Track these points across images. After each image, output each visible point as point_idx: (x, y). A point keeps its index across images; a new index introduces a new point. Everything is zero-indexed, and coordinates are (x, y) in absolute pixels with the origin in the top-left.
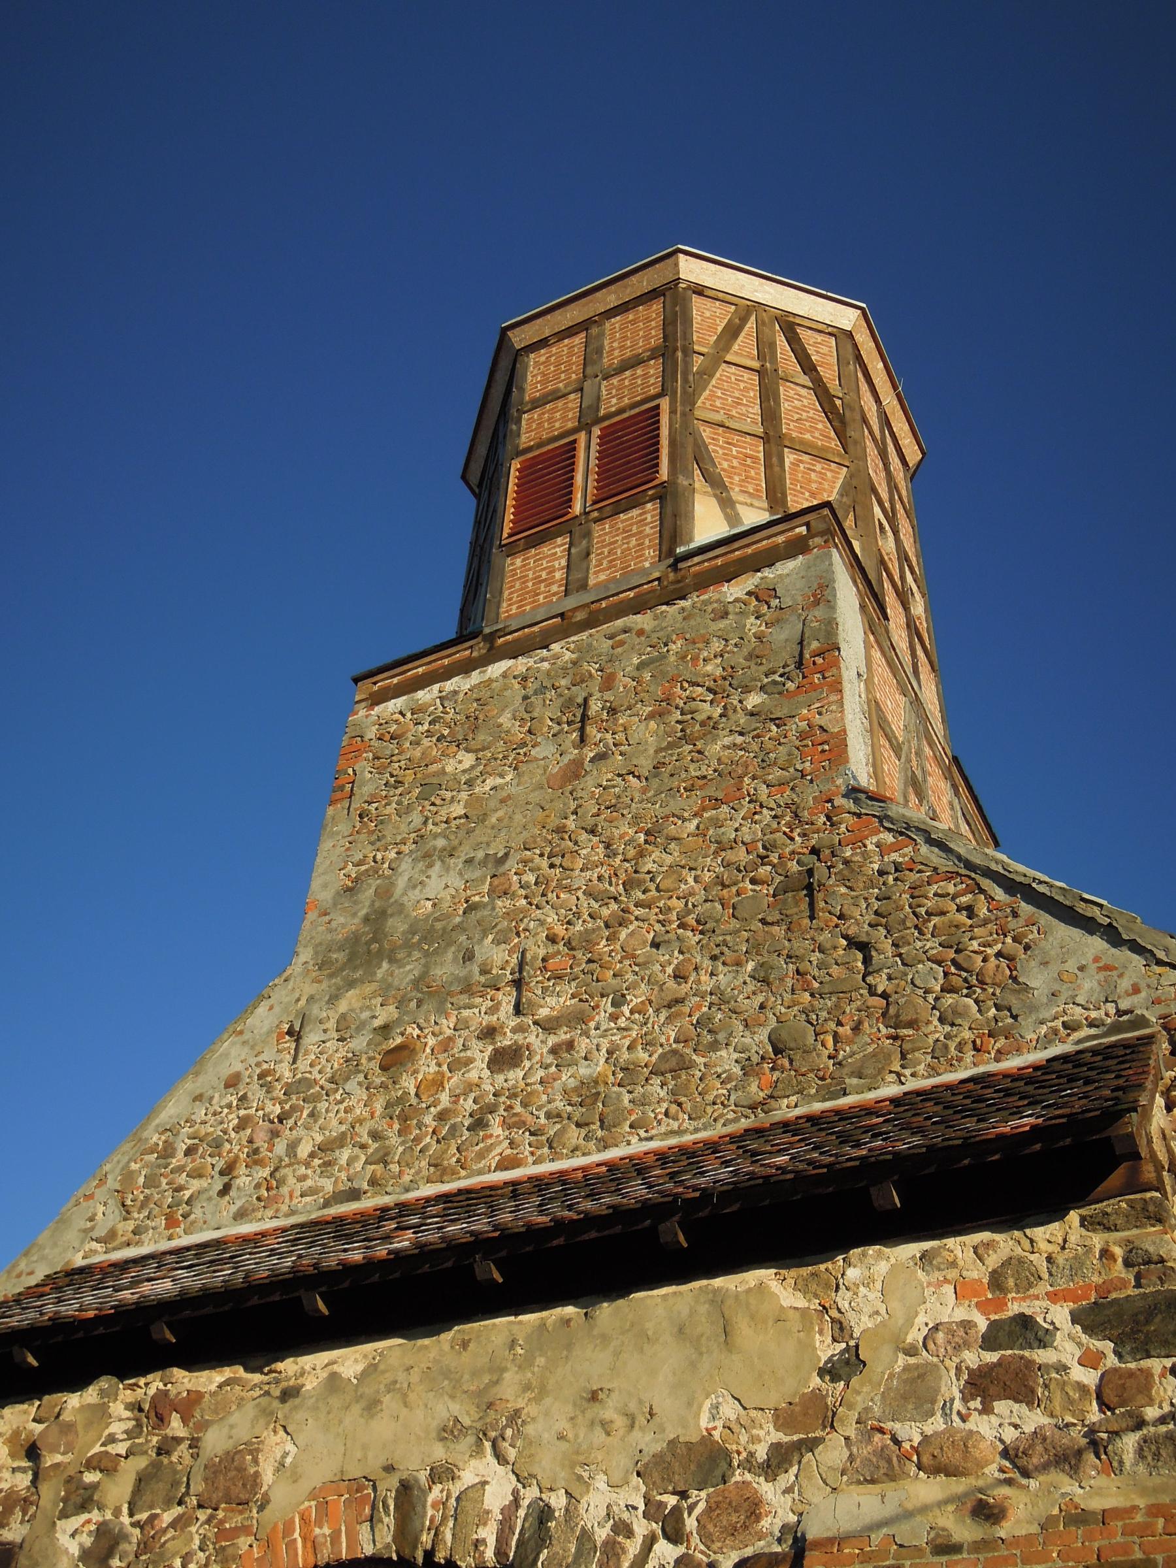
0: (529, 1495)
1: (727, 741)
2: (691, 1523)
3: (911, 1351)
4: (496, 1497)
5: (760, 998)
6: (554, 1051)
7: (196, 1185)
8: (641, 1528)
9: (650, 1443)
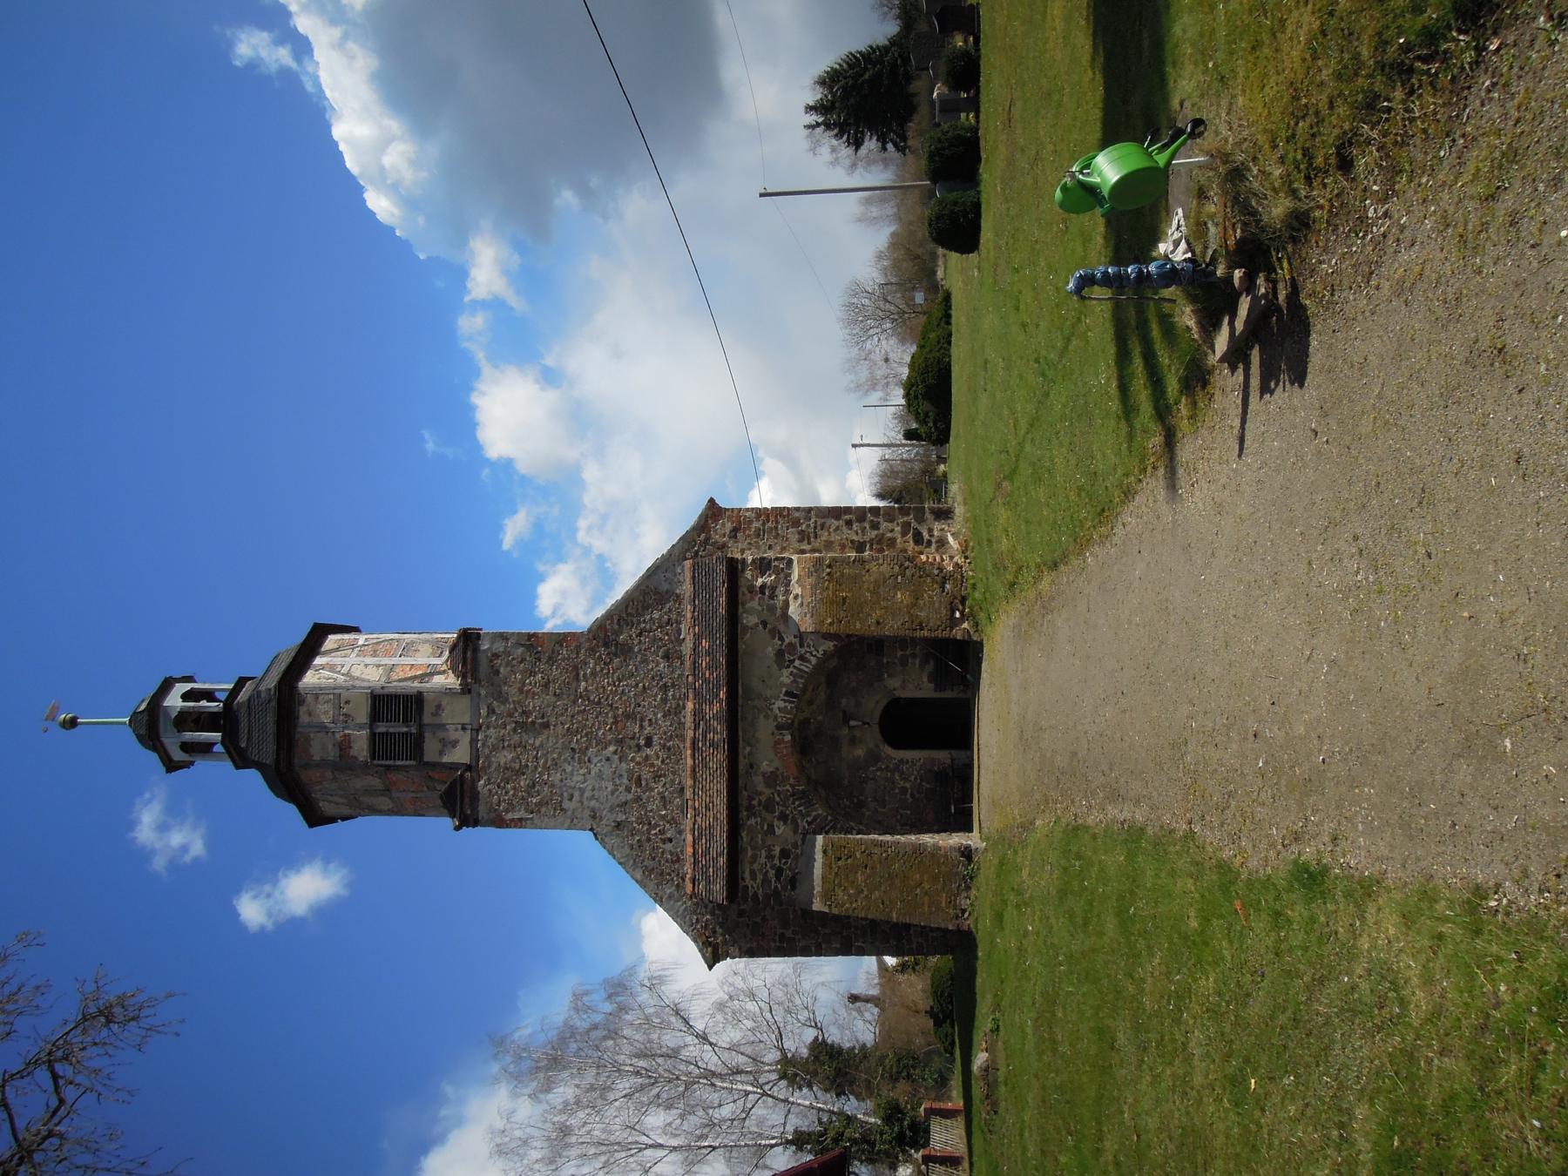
0: (782, 696)
8: (791, 669)
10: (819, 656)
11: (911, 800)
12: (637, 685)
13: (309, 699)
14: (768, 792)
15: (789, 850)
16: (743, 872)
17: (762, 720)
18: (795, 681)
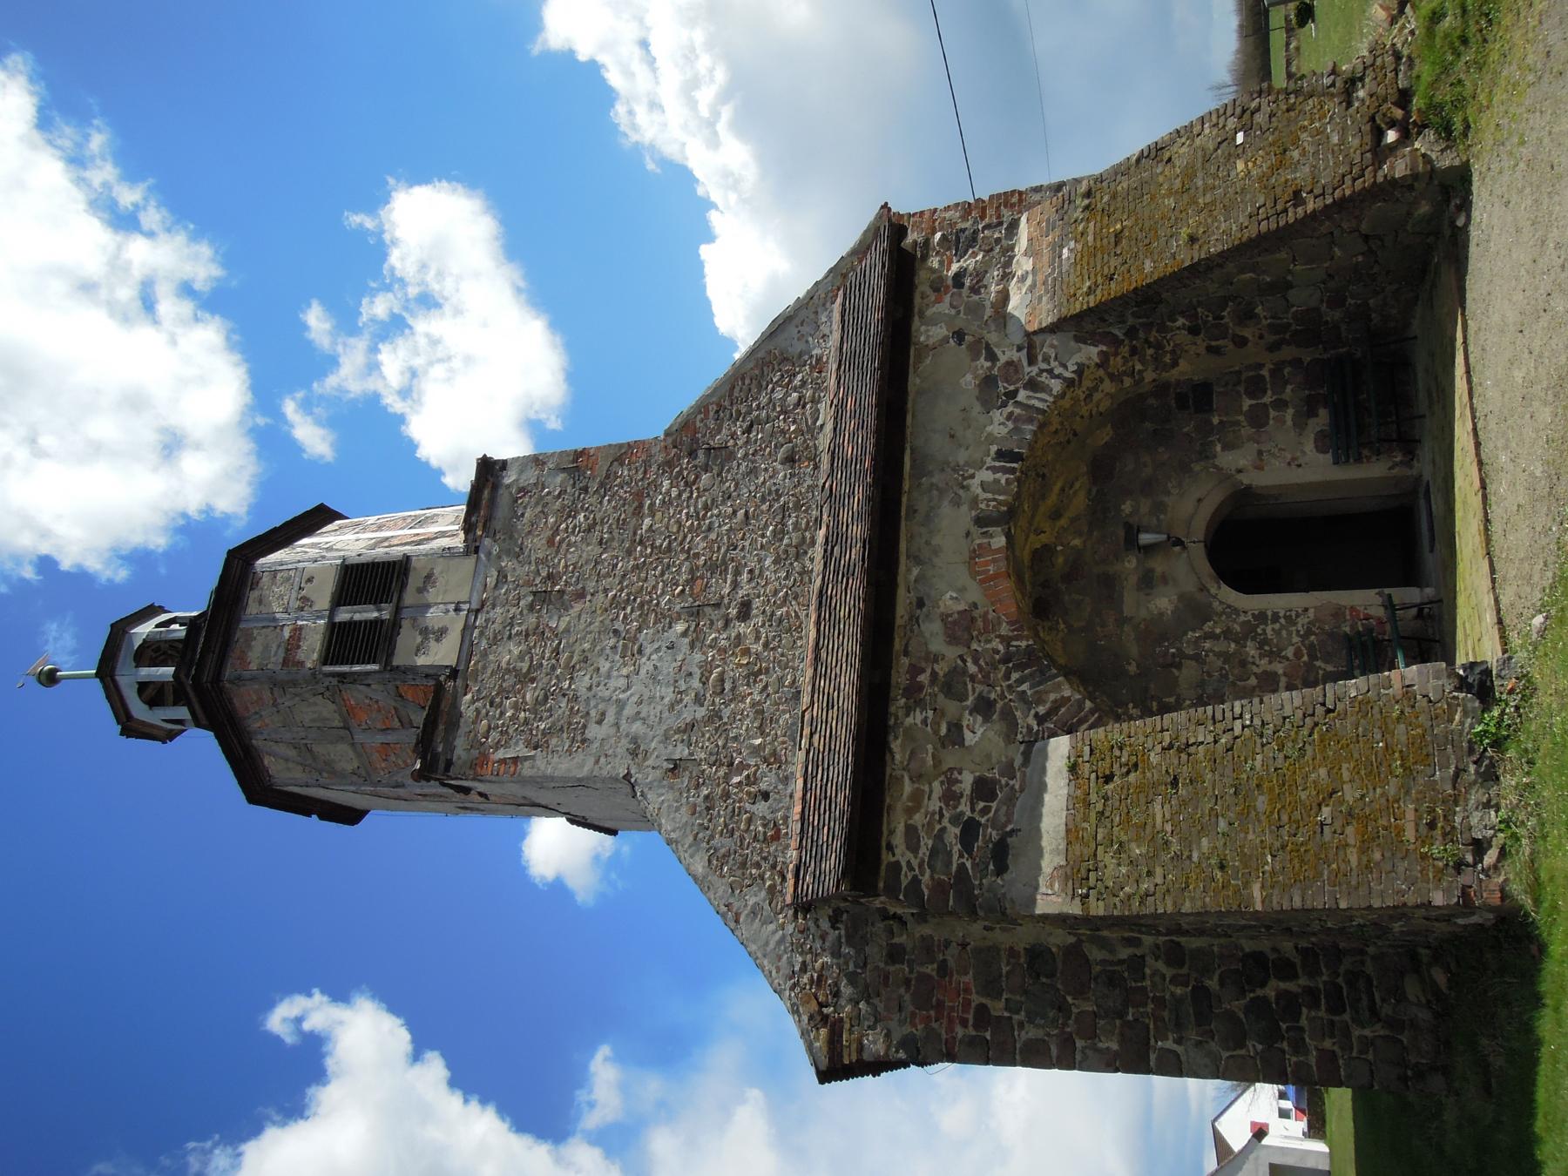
0: (989, 462)
2: (1012, 388)
4: (987, 476)
8: (1010, 408)
10: (1068, 375)
12: (735, 512)
13: (266, 579)
14: (952, 652)
15: (994, 782)
16: (891, 832)
17: (946, 509)
18: (1016, 430)
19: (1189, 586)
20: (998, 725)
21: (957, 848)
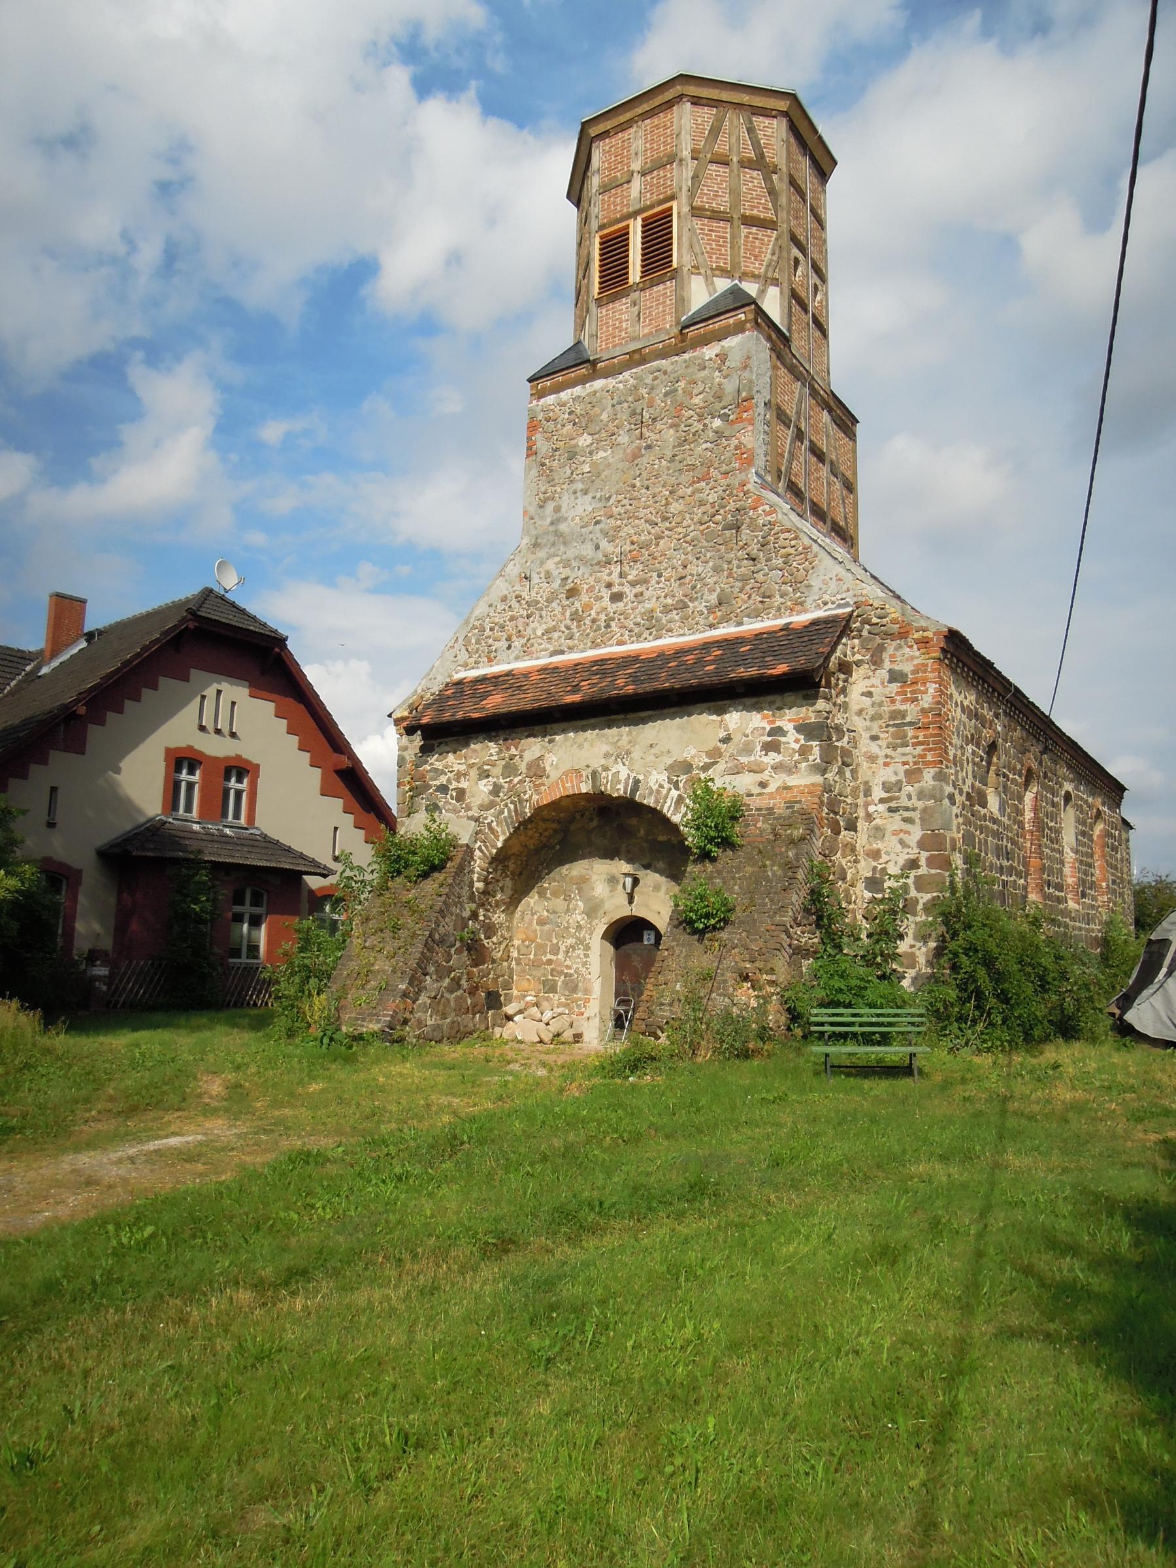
0: (632, 775)
1: (704, 446)
2: (681, 785)
3: (747, 736)
4: (622, 776)
5: (715, 579)
6: (636, 596)
7: (497, 644)
8: (666, 786)
9: (669, 761)
11: (544, 959)
14: (523, 768)
16: (446, 744)
19: (608, 906)
20: (486, 801)
21: (438, 783)
